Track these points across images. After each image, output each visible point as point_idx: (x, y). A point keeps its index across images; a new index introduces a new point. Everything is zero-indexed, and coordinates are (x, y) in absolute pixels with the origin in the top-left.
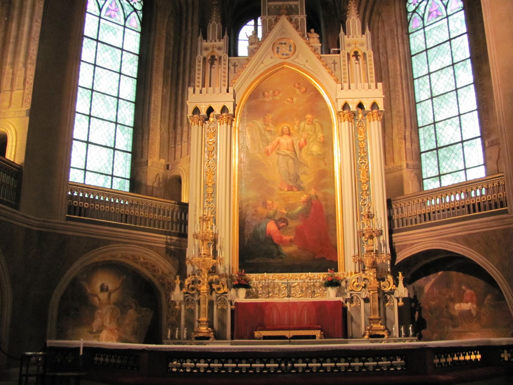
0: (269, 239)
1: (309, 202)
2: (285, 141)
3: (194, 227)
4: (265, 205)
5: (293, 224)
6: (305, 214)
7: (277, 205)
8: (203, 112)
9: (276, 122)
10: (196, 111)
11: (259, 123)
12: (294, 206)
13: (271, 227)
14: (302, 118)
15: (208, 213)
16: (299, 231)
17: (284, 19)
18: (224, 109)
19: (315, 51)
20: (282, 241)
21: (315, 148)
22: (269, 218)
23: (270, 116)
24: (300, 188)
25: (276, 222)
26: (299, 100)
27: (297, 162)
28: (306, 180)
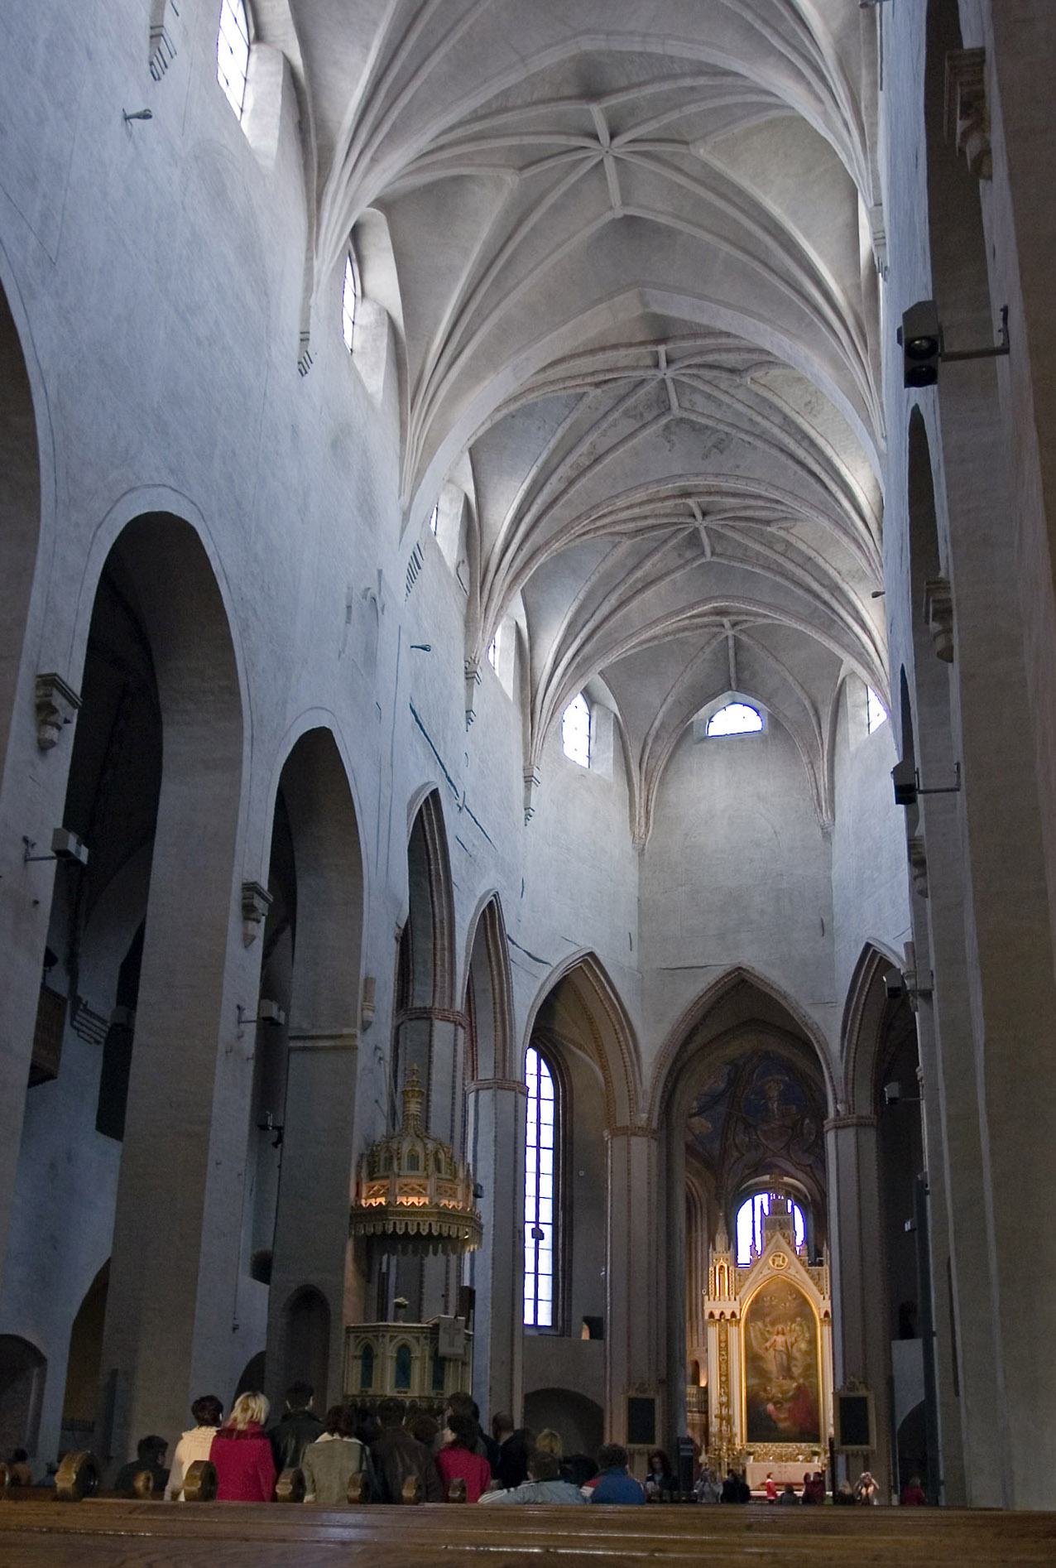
0: (769, 1416)
1: (799, 1388)
2: (780, 1339)
3: (714, 1408)
4: (765, 1390)
5: (787, 1405)
6: (795, 1398)
7: (774, 1390)
8: (717, 1317)
9: (773, 1324)
10: (712, 1315)
11: (760, 1324)
12: (787, 1392)
13: (770, 1407)
14: (793, 1321)
15: (724, 1399)
16: (790, 1411)
17: (778, 1235)
18: (733, 1315)
19: (803, 1264)
20: (781, 1420)
21: (803, 1346)
22: (769, 1400)
23: (768, 1320)
24: (792, 1378)
25: (775, 1404)
26: (790, 1305)
27: (789, 1357)
28: (796, 1371)
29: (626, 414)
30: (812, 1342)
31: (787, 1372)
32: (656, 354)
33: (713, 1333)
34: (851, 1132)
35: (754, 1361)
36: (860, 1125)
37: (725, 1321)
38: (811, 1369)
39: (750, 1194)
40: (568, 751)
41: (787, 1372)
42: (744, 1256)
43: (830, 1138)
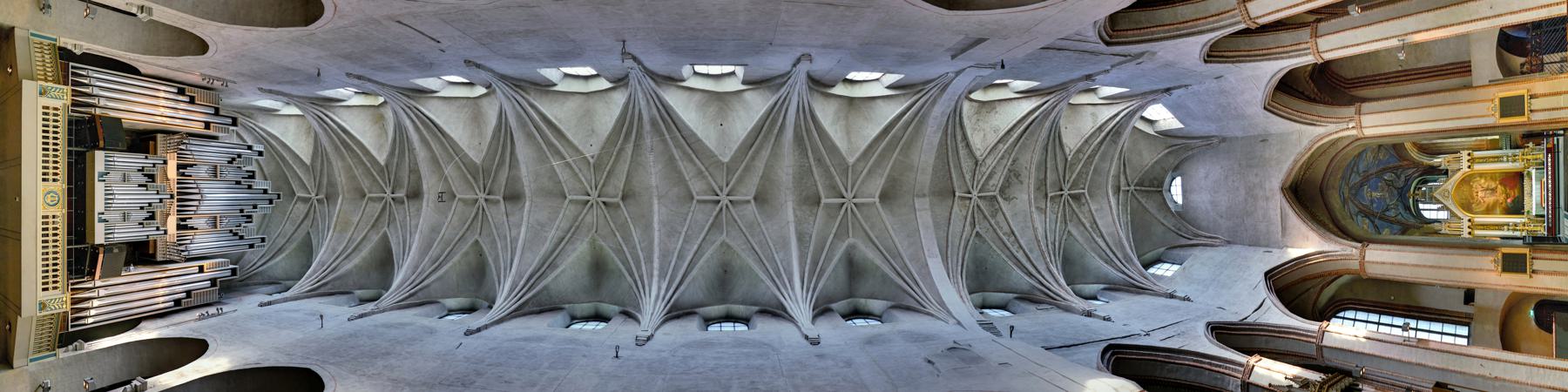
7: (1501, 198)
26: (1465, 188)
29: (994, 216)
30: (1481, 175)
31: (1494, 190)
32: (962, 198)
33: (1477, 232)
34: (1363, 118)
35: (1489, 211)
36: (1359, 113)
37: (1473, 226)
38: (1491, 176)
39: (1418, 210)
40: (1169, 274)
41: (1494, 190)
42: (1443, 215)
43: (1368, 132)
